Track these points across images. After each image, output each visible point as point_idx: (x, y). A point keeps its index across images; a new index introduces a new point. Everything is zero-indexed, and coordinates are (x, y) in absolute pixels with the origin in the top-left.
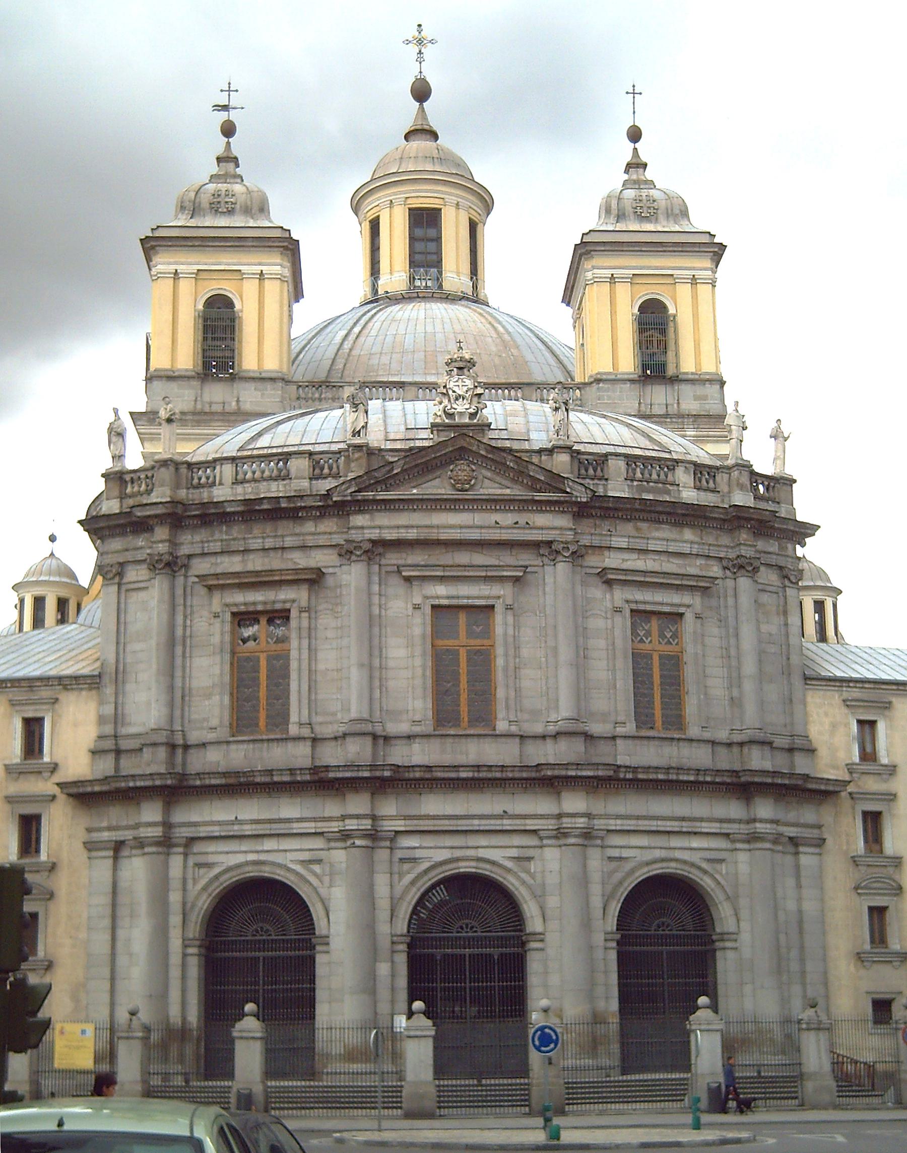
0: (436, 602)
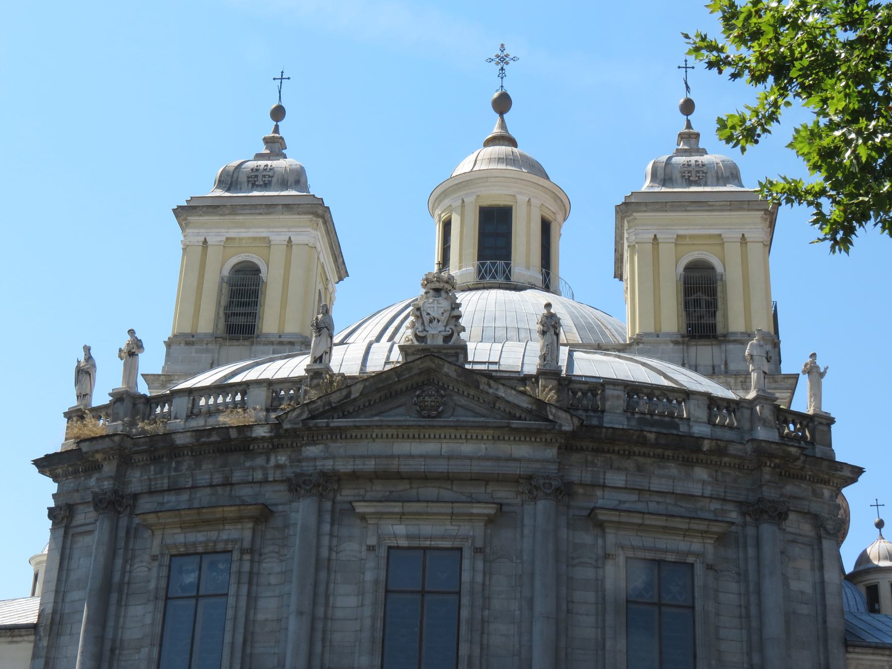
0: (393, 543)
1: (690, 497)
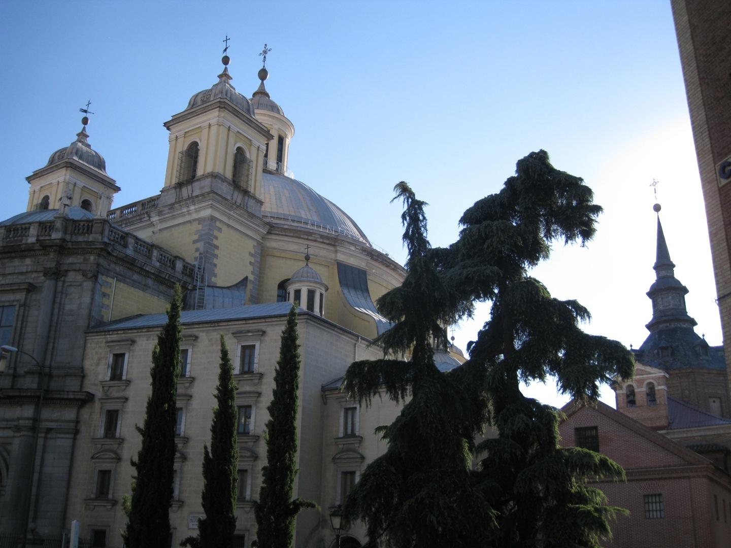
1: (22, 273)
